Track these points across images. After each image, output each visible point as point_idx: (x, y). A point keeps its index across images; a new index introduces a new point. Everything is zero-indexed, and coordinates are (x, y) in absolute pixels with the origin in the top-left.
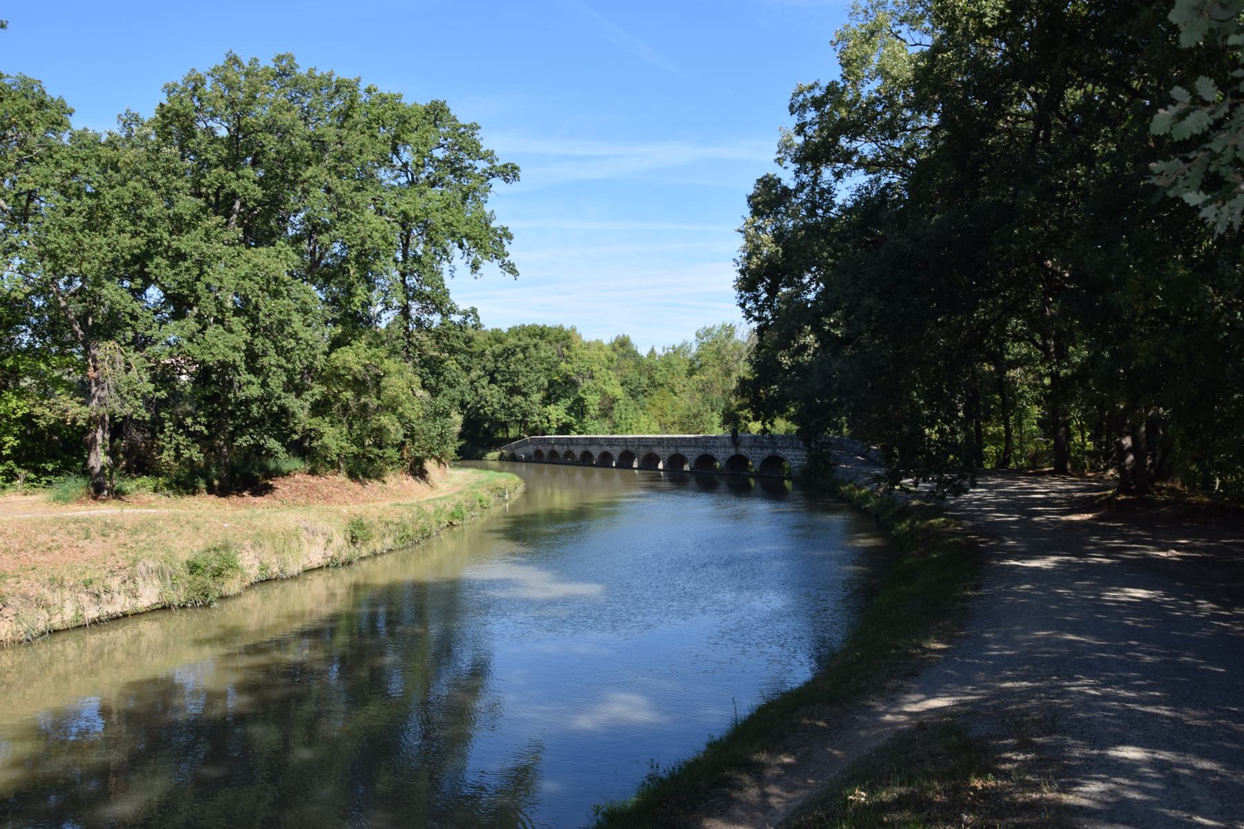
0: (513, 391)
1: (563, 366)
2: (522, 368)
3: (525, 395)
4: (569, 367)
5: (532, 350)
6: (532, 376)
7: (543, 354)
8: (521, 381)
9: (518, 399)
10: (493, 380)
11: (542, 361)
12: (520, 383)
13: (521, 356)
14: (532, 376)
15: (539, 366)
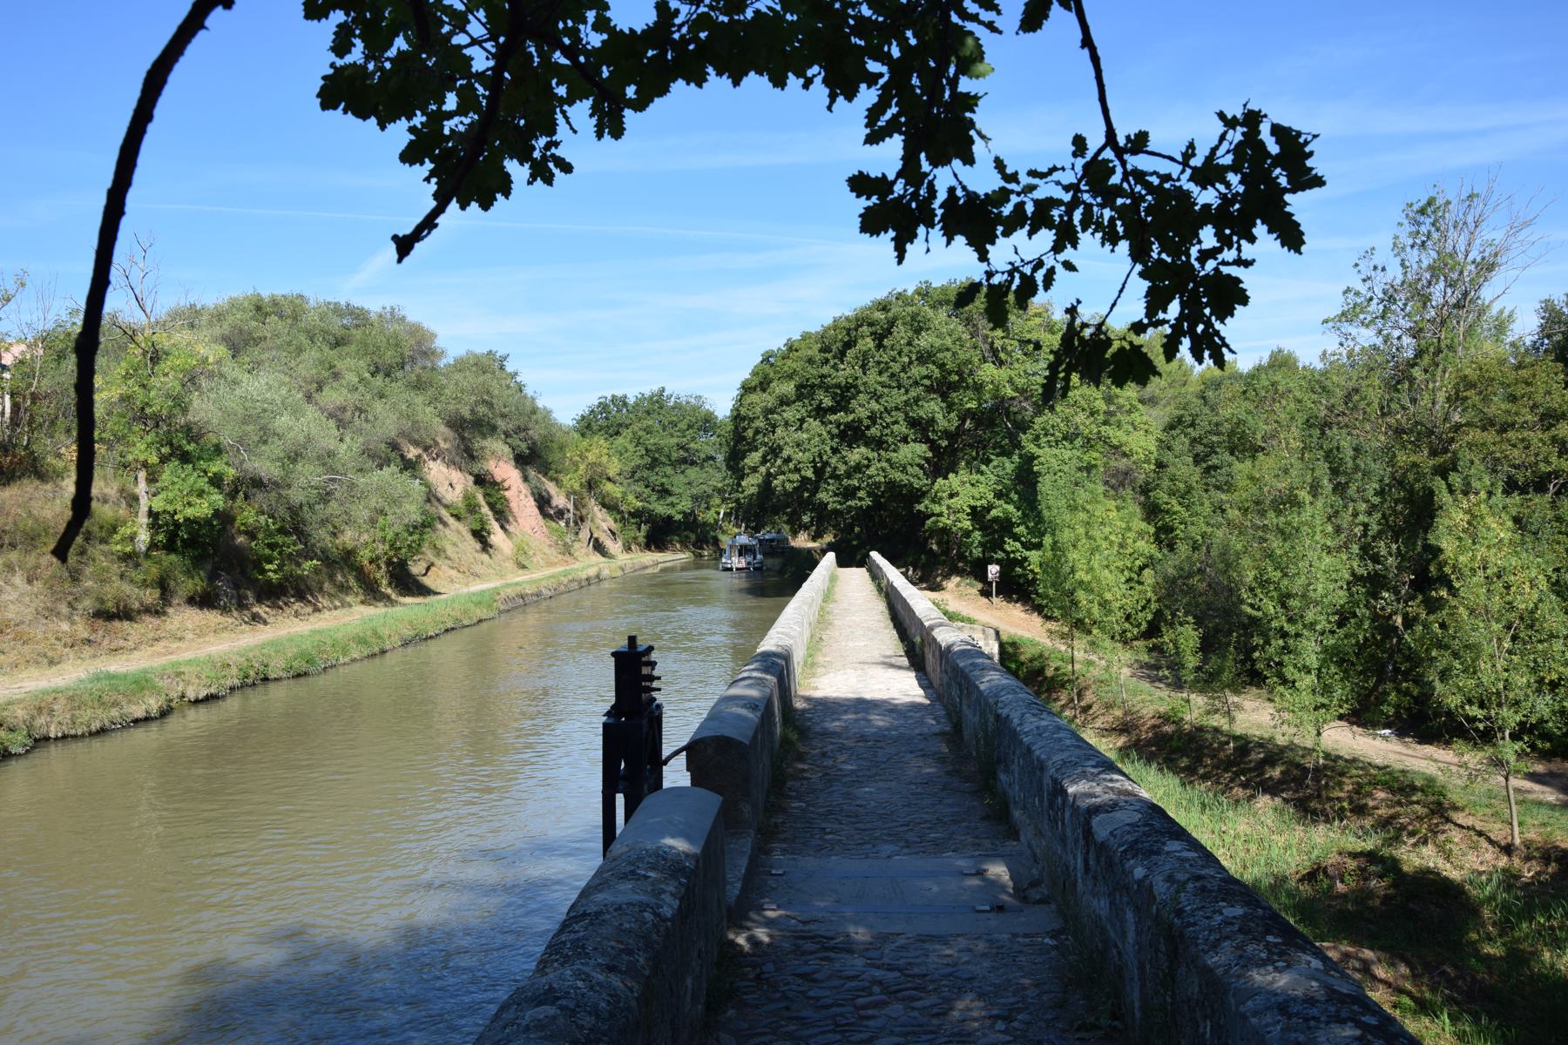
0: (852, 434)
1: (987, 372)
2: (872, 377)
3: (878, 444)
4: (1002, 374)
5: (901, 333)
6: (898, 397)
7: (925, 341)
8: (862, 408)
9: (857, 454)
10: (820, 412)
11: (924, 358)
12: (862, 413)
13: (869, 343)
14: (898, 397)
15: (917, 371)
